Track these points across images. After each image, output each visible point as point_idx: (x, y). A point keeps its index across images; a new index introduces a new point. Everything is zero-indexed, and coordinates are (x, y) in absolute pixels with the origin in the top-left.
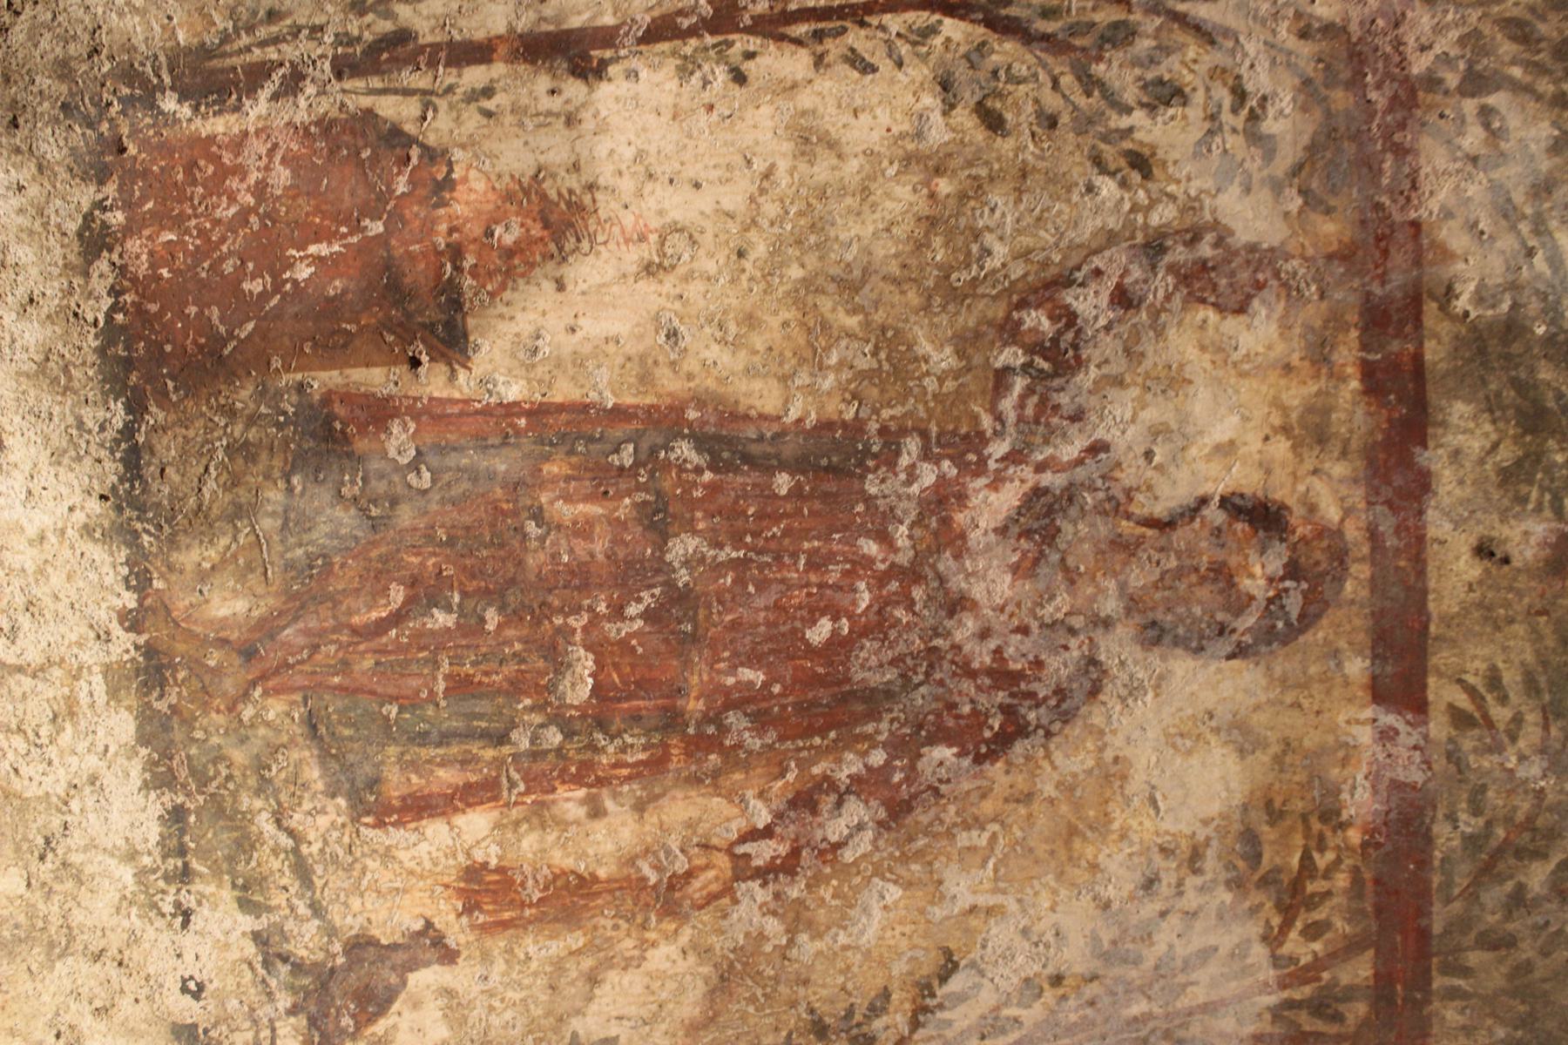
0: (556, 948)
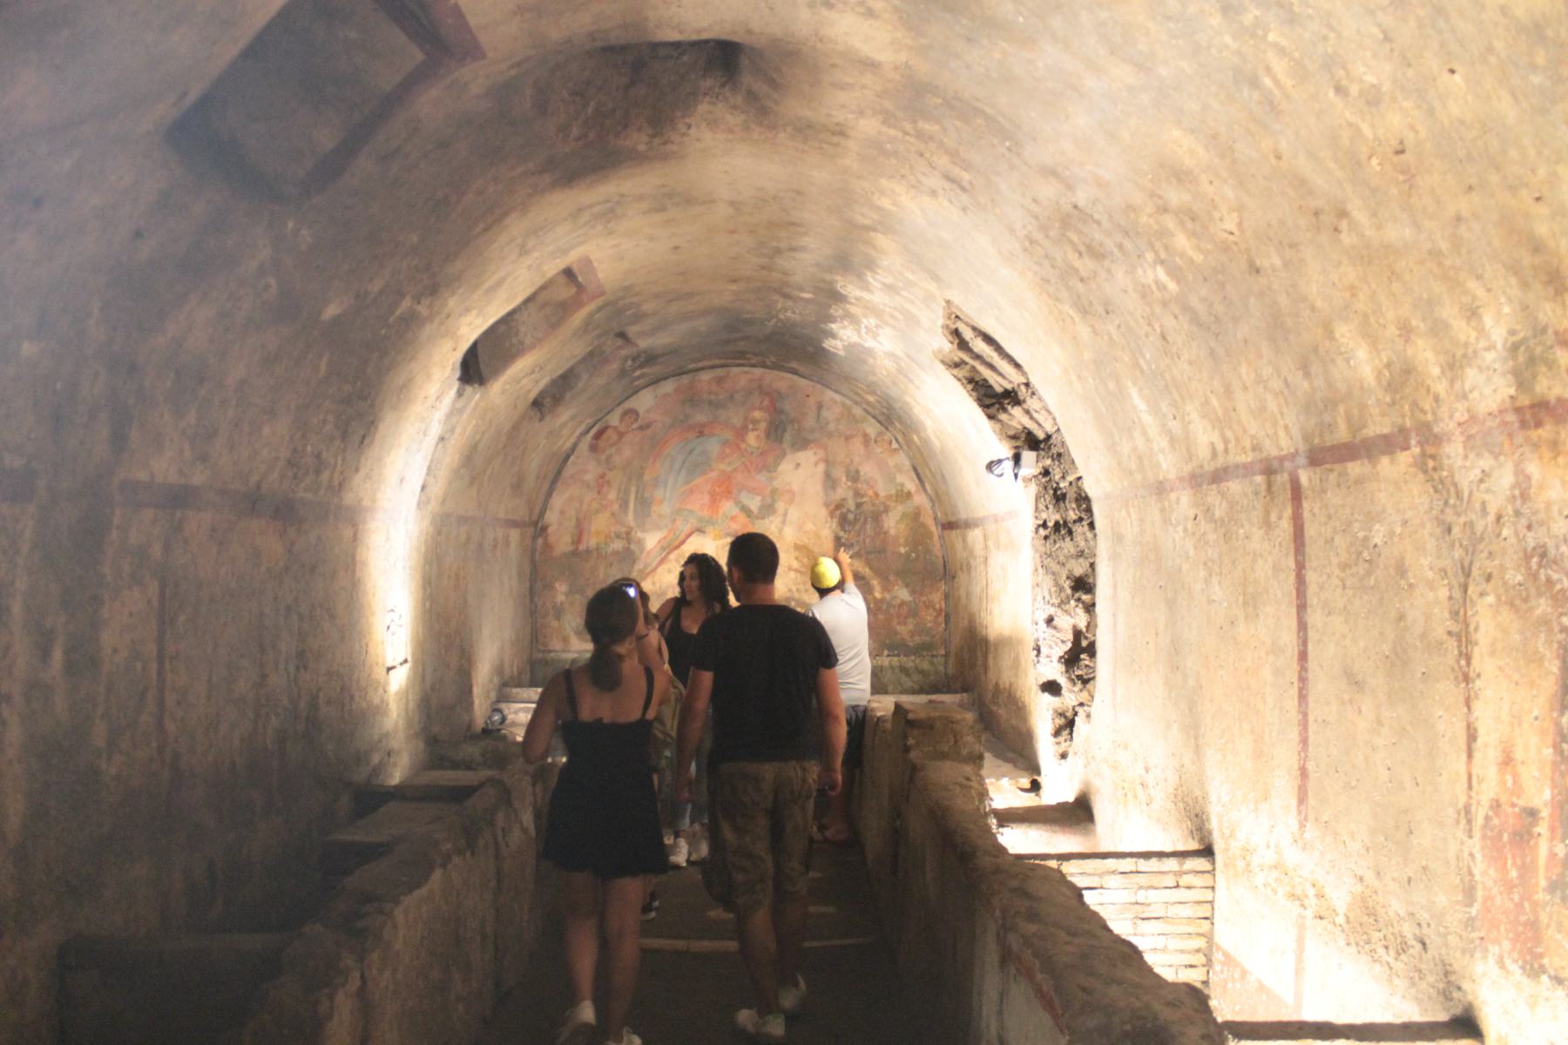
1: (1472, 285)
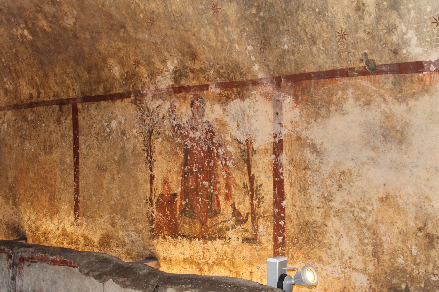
0: (233, 189)
1: (166, 54)
